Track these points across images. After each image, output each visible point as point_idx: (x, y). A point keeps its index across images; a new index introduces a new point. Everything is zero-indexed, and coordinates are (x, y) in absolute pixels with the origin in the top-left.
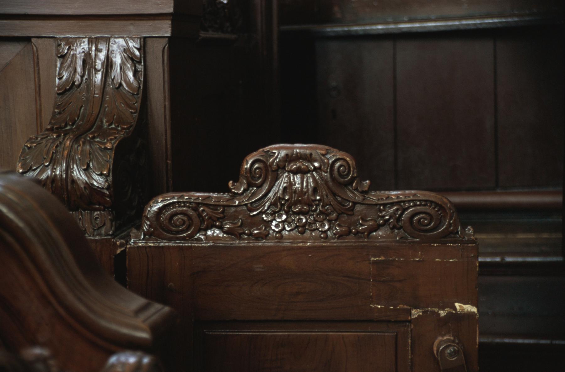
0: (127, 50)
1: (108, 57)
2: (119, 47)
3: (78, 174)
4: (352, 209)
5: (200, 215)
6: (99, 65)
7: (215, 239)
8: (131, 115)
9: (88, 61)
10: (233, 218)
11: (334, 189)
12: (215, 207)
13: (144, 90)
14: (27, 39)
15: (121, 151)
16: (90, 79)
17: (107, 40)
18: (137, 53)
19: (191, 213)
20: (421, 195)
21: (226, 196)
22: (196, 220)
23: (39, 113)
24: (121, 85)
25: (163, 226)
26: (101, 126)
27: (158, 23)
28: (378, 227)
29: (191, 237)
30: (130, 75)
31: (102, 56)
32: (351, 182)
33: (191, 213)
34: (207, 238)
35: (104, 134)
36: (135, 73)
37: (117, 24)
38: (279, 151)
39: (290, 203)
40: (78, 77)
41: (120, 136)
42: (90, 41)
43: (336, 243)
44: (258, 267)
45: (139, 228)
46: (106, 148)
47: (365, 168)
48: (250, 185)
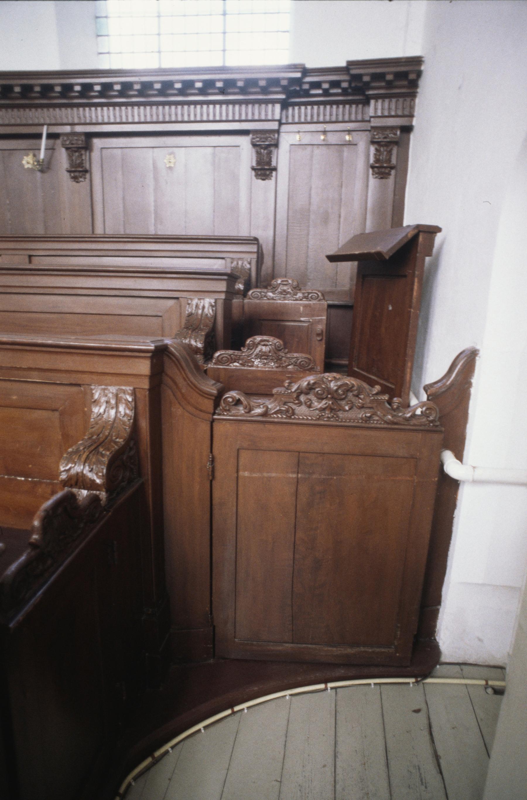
0: (210, 303)
2: (207, 302)
3: (193, 343)
4: (281, 359)
5: (231, 358)
6: (201, 307)
7: (236, 366)
8: (211, 325)
9: (197, 306)
10: (242, 359)
11: (276, 352)
12: (236, 355)
13: (215, 317)
14: (177, 298)
15: (207, 336)
19: (229, 357)
20: (304, 355)
22: (230, 360)
25: (219, 361)
27: (220, 294)
28: (289, 365)
29: (228, 365)
32: (280, 350)
33: (229, 357)
34: (234, 366)
35: (202, 330)
36: (213, 310)
37: (206, 294)
38: (258, 338)
39: (262, 356)
41: (207, 331)
43: (275, 369)
44: (249, 376)
45: (212, 361)
47: (286, 345)
48: (248, 349)
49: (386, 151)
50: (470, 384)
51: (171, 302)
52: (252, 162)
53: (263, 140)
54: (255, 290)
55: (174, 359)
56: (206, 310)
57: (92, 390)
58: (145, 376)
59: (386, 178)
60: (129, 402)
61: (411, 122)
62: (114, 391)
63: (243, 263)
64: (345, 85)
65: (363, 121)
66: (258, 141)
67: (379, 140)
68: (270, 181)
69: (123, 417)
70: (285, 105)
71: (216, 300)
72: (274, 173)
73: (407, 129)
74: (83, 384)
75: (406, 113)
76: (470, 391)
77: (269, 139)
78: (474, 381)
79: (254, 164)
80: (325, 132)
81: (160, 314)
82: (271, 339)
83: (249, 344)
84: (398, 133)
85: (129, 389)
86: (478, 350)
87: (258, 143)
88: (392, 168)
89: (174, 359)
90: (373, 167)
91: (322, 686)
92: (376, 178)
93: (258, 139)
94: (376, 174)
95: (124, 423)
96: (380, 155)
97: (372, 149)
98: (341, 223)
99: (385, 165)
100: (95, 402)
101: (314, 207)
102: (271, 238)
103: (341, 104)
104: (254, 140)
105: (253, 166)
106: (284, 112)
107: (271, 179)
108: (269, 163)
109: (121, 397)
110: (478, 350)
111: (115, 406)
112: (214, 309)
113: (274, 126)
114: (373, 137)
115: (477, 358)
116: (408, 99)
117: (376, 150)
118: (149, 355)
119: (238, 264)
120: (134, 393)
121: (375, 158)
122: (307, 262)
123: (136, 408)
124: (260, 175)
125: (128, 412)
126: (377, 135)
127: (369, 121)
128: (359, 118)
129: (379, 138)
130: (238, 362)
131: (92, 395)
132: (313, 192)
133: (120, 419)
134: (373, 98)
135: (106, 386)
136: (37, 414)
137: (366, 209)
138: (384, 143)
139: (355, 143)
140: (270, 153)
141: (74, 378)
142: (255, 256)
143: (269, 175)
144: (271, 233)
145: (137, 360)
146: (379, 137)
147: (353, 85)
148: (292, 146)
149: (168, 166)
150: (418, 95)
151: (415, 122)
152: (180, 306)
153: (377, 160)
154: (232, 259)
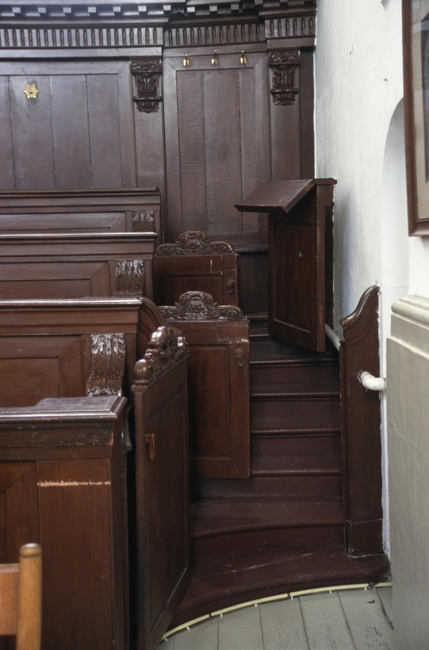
0: (139, 264)
1: (133, 266)
2: (135, 263)
9: (126, 267)
13: (144, 277)
16: (127, 273)
17: (132, 261)
18: (142, 265)
21: (175, 307)
23: (110, 284)
24: (137, 274)
26: (133, 288)
27: (148, 255)
30: (140, 271)
31: (131, 265)
34: (170, 320)
36: (141, 271)
40: (123, 272)
42: (127, 261)
46: (140, 294)
49: (287, 74)
50: (376, 316)
51: (99, 266)
52: (133, 92)
53: (145, 68)
54: (161, 246)
55: (148, 311)
56: (135, 271)
57: (91, 337)
58: (134, 324)
59: (291, 104)
60: (121, 344)
61: (313, 42)
62: (109, 337)
63: (145, 216)
64: (235, 7)
65: (258, 42)
66: (139, 69)
67: (278, 63)
68: (156, 113)
69: (118, 356)
70: (166, 27)
71: (144, 261)
72: (160, 104)
73: (310, 50)
74: (83, 334)
75: (307, 32)
76: (377, 321)
77: (153, 66)
78: (379, 312)
79: (136, 94)
80: (216, 56)
81: (88, 277)
82: (201, 294)
83: (182, 299)
84: (299, 53)
85: (121, 335)
86: (379, 288)
87: (140, 72)
88: (295, 93)
89: (148, 311)
90: (274, 93)
91: (285, 595)
92: (278, 104)
93: (139, 67)
94: (278, 100)
95: (119, 360)
96: (281, 79)
97: (271, 73)
98: (243, 156)
99: (287, 90)
100: (94, 346)
101: (208, 141)
102: (162, 179)
103: (232, 24)
104: (134, 69)
105: (136, 98)
106: (167, 33)
107: (157, 111)
108: (154, 93)
109: (115, 341)
110: (379, 288)
111: (110, 348)
112: (143, 269)
113: (156, 51)
114: (271, 60)
115: (379, 294)
116: (307, 19)
117: (275, 73)
118: (138, 308)
119: (140, 217)
120: (124, 338)
121: (275, 82)
122: (206, 204)
123: (126, 349)
124: (143, 107)
125: (121, 351)
126: (275, 58)
127: (266, 42)
128: (254, 39)
129: (278, 61)
130: (173, 317)
131: (91, 341)
132: (207, 122)
133: (116, 358)
134: (267, 19)
135: (102, 334)
136: (39, 363)
137: (270, 145)
138: (284, 67)
139: (251, 66)
140: (154, 82)
141: (75, 331)
142: (158, 208)
143: (154, 106)
144: (162, 172)
145: (127, 313)
146: (278, 59)
147: (244, 7)
148: (178, 72)
149: (29, 97)
150: (317, 14)
151: (315, 44)
152: (109, 269)
153: (278, 86)
154: (133, 212)
